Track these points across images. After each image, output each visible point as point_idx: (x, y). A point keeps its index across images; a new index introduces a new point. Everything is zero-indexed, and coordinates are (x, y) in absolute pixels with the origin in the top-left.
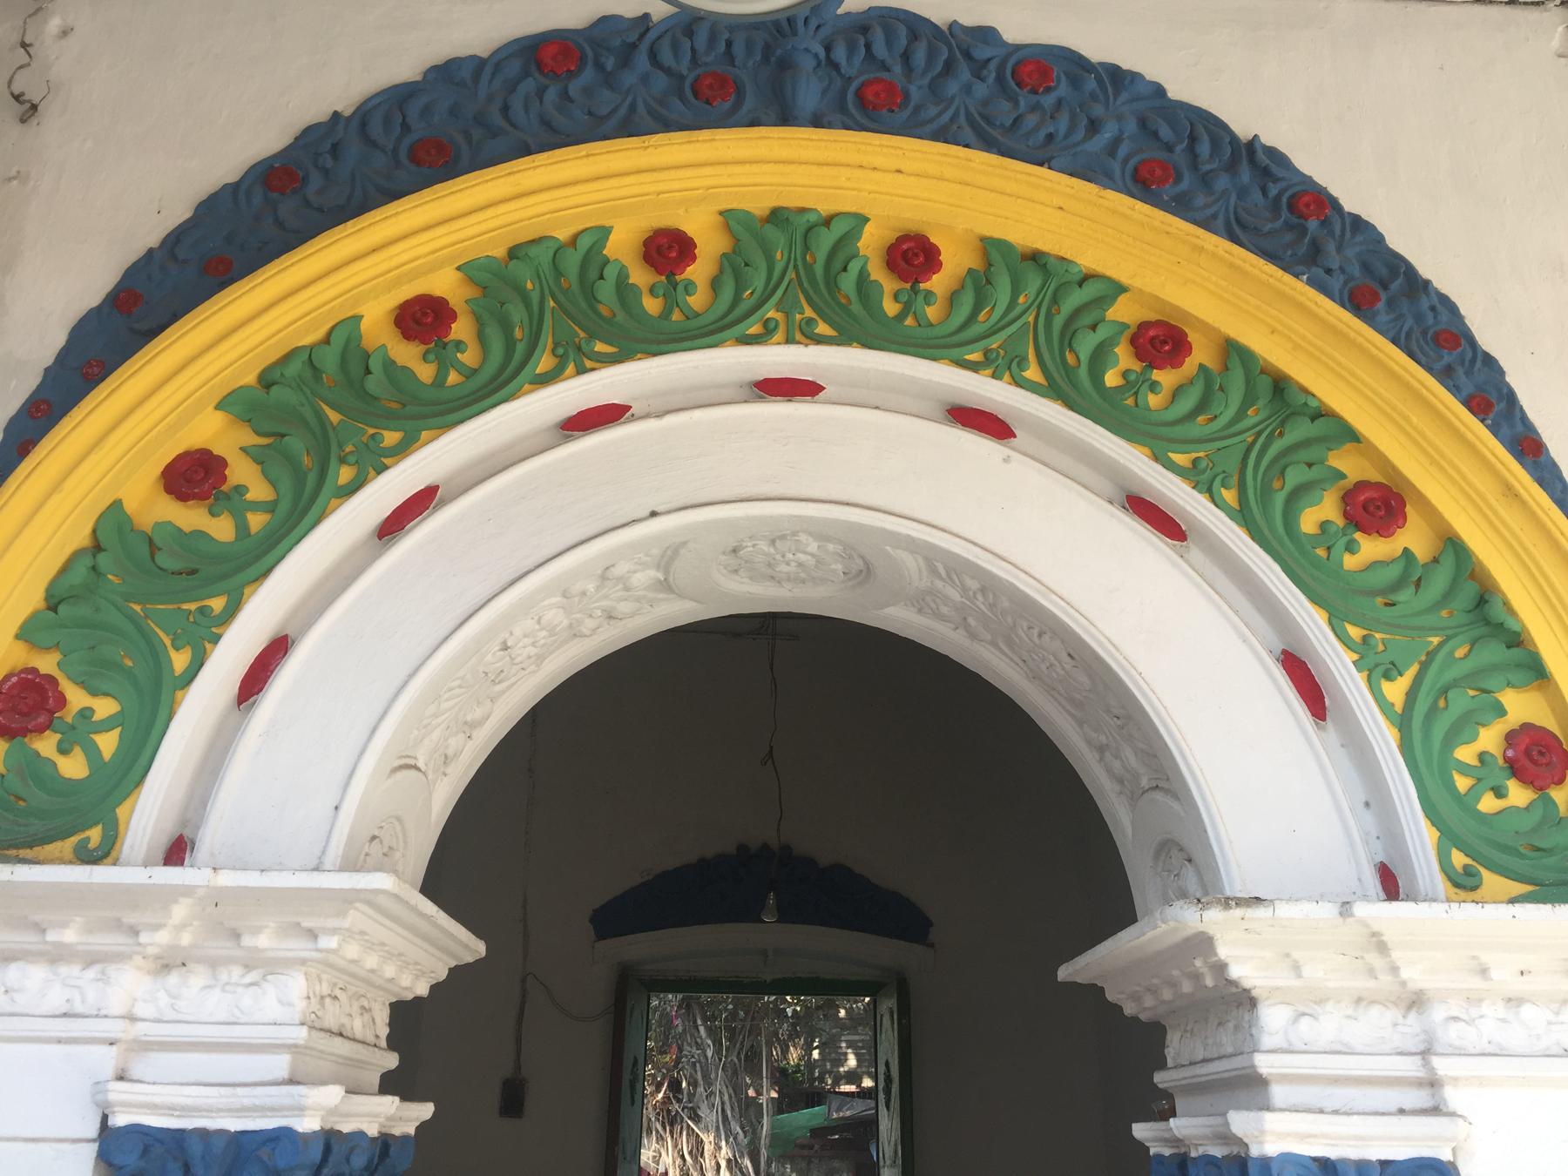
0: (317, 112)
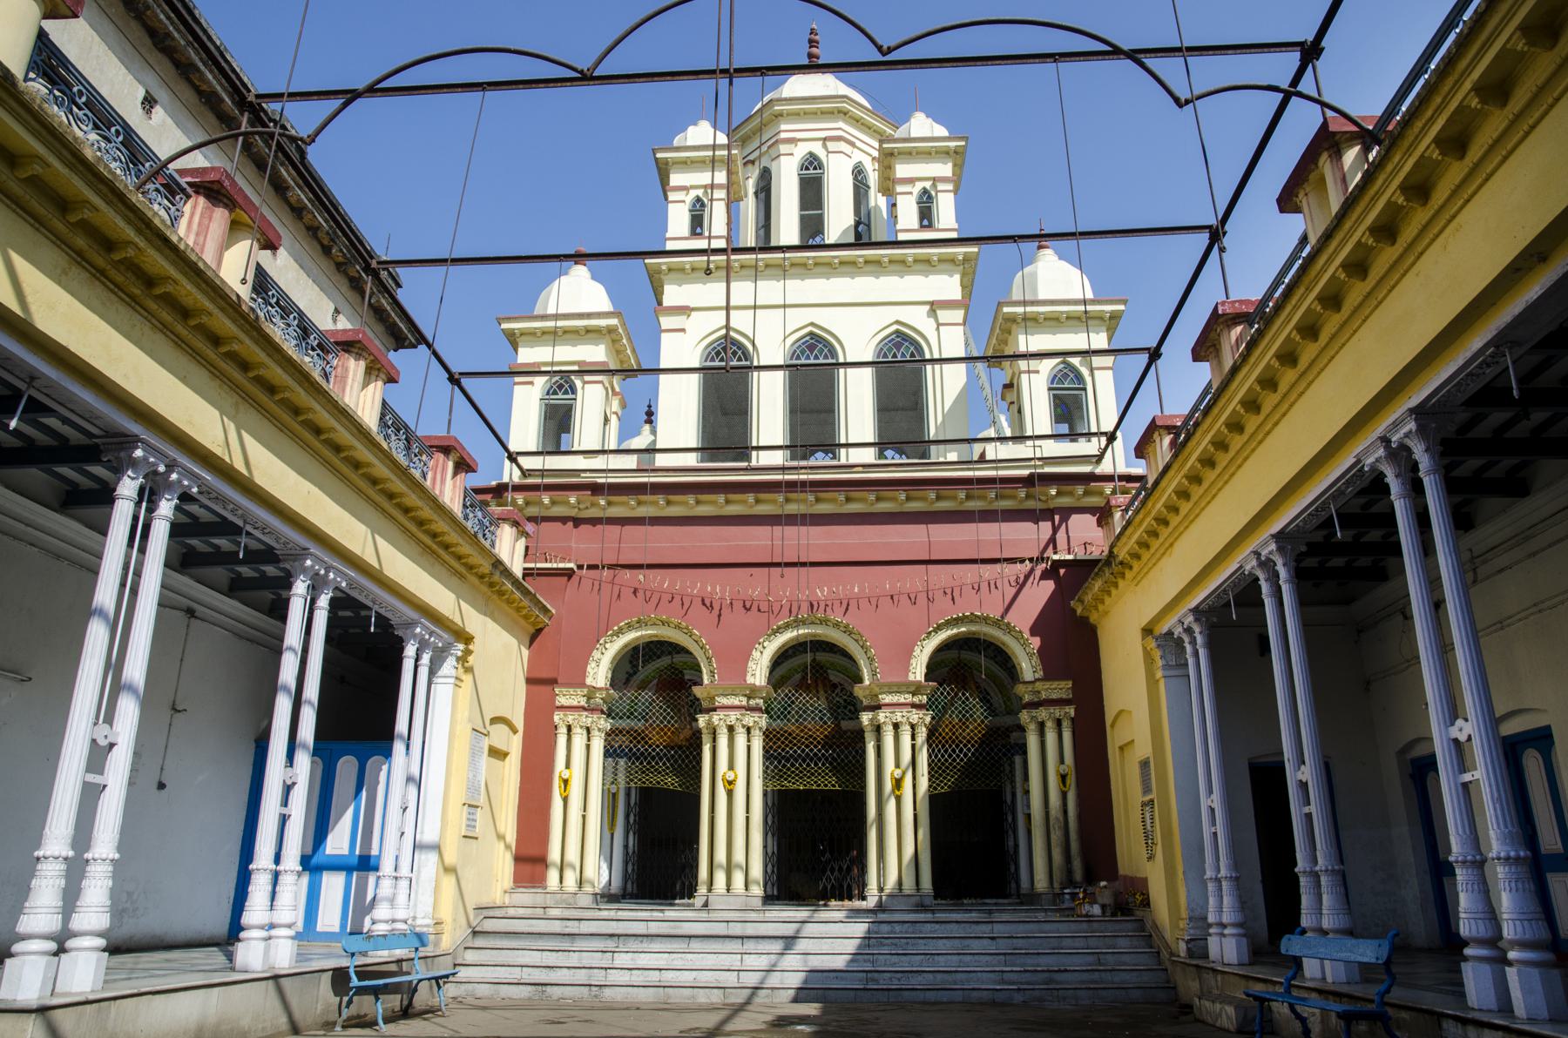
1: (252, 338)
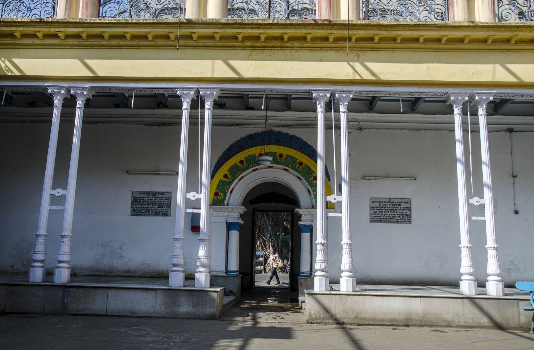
0: (231, 143)
1: (336, 29)
